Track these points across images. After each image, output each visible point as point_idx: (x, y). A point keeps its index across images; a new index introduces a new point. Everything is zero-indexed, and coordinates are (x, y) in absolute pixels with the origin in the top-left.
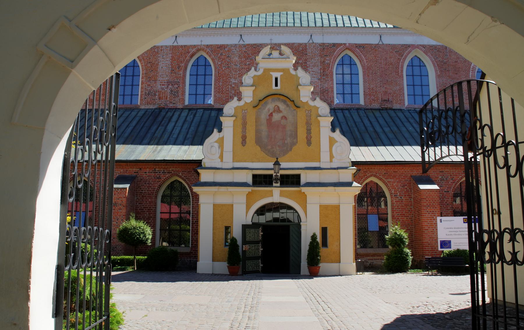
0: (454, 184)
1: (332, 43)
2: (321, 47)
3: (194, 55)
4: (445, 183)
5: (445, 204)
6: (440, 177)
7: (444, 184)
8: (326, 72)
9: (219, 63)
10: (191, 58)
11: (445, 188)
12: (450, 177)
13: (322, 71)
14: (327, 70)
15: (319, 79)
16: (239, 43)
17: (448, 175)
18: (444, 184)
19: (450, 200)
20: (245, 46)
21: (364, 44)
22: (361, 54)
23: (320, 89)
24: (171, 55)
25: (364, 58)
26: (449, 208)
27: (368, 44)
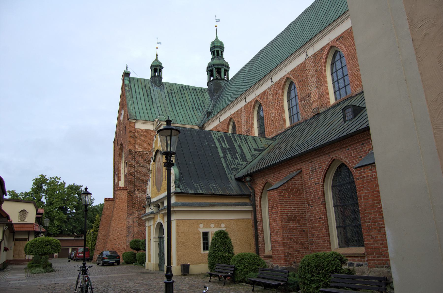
0: (322, 173)
1: (320, 49)
2: (314, 58)
3: (255, 106)
4: (315, 173)
5: (317, 199)
6: (310, 169)
7: (314, 176)
8: (320, 78)
9: (264, 106)
10: (254, 109)
11: (316, 180)
12: (318, 166)
13: (317, 78)
14: (320, 76)
15: (317, 87)
16: (272, 85)
17: (317, 164)
18: (314, 176)
19: (320, 192)
20: (275, 83)
21: (342, 34)
22: (341, 45)
23: (318, 95)
24: (245, 112)
25: (343, 47)
26: (320, 203)
27: (345, 32)
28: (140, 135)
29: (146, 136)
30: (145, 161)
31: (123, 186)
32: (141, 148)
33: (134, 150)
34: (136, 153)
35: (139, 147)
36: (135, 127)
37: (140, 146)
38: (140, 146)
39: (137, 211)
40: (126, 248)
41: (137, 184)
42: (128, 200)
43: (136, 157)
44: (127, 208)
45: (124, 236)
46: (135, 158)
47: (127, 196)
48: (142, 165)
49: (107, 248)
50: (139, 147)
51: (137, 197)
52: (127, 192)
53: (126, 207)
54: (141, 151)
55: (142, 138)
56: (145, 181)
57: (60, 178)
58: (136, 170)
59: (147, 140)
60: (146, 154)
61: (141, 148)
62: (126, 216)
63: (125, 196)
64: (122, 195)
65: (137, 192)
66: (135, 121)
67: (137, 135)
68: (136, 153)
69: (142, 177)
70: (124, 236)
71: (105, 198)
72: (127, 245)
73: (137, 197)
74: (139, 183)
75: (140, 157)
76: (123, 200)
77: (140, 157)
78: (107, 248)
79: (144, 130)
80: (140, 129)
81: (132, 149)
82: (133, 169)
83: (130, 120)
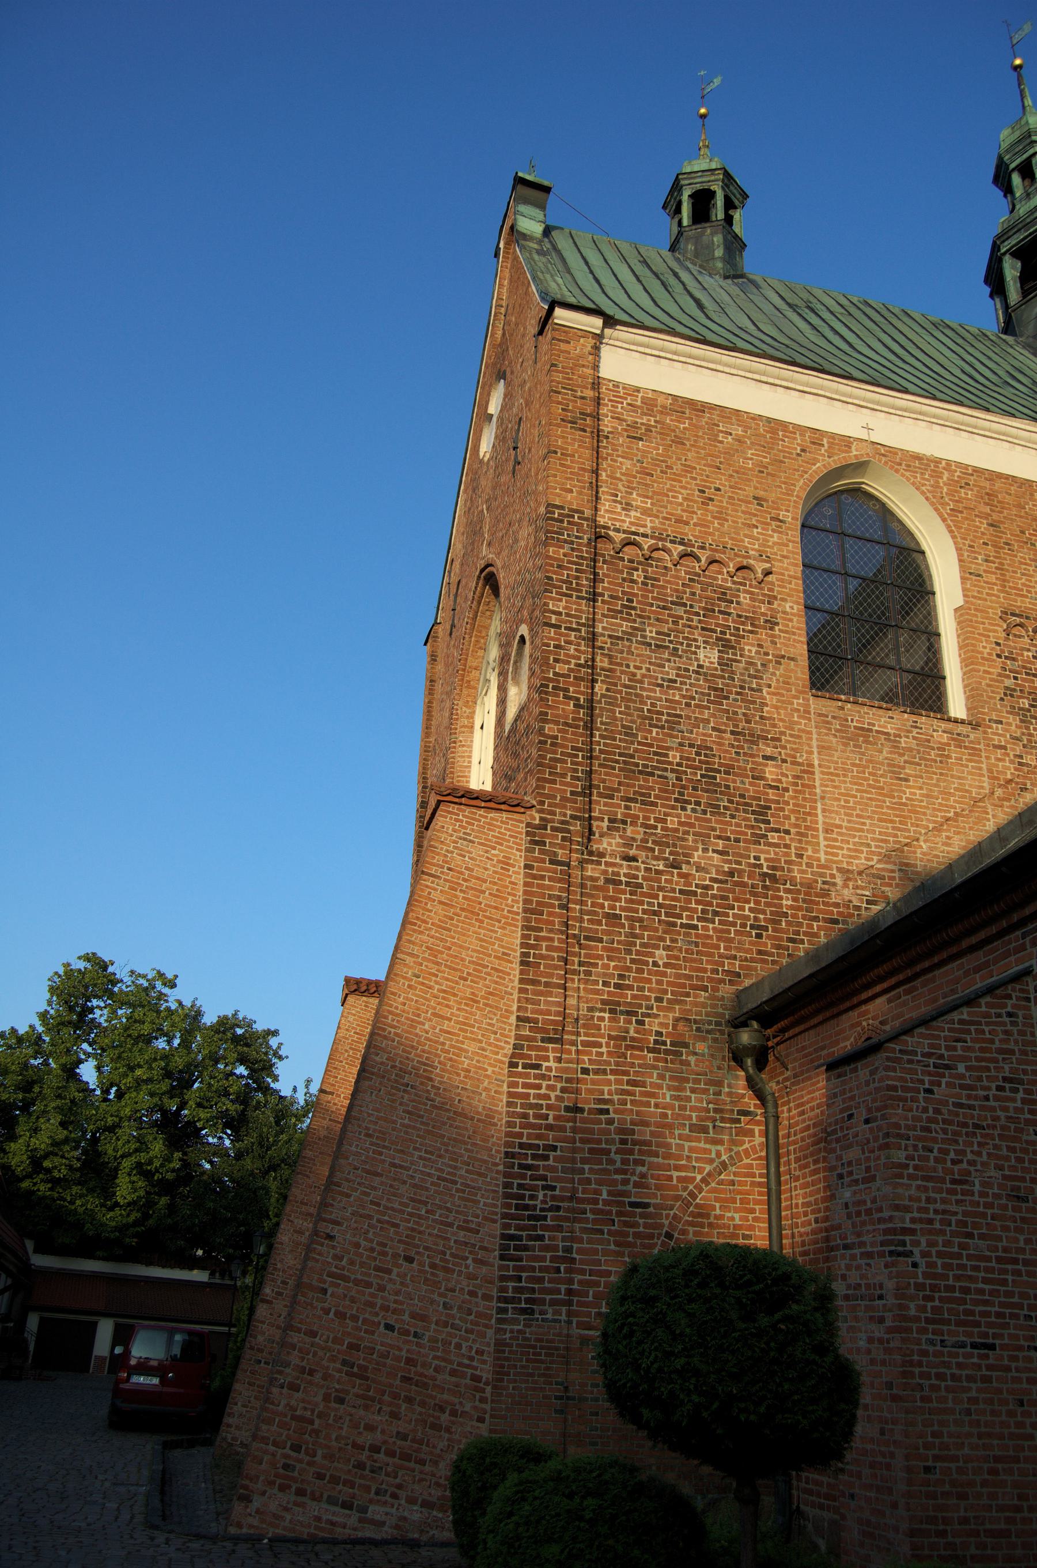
28: (634, 426)
29: (679, 442)
30: (680, 611)
31: (488, 787)
32: (646, 512)
33: (588, 513)
34: (608, 538)
35: (628, 507)
36: (596, 367)
37: (636, 500)
38: (636, 500)
39: (612, 1007)
40: (486, 1371)
41: (606, 777)
42: (526, 902)
43: (603, 570)
44: (515, 969)
45: (472, 1239)
46: (595, 580)
47: (519, 859)
48: (651, 633)
49: (294, 1358)
50: (628, 507)
51: (608, 881)
52: (522, 828)
53: (505, 957)
54: (642, 530)
55: (652, 448)
56: (674, 756)
57: (176, 976)
58: (602, 662)
59: (688, 469)
60: (683, 556)
61: (646, 512)
62: (509, 1049)
63: (506, 863)
64: (477, 851)
65: (609, 844)
66: (595, 323)
67: (607, 424)
68: (599, 536)
69: (651, 719)
70: (472, 1239)
71: (348, 980)
72: (500, 1344)
73: (608, 881)
74: (630, 771)
75: (638, 576)
76: (485, 899)
77: (638, 576)
78: (294, 1358)
79: (661, 400)
80: (638, 390)
81: (574, 498)
82: (576, 652)
83: (558, 312)
